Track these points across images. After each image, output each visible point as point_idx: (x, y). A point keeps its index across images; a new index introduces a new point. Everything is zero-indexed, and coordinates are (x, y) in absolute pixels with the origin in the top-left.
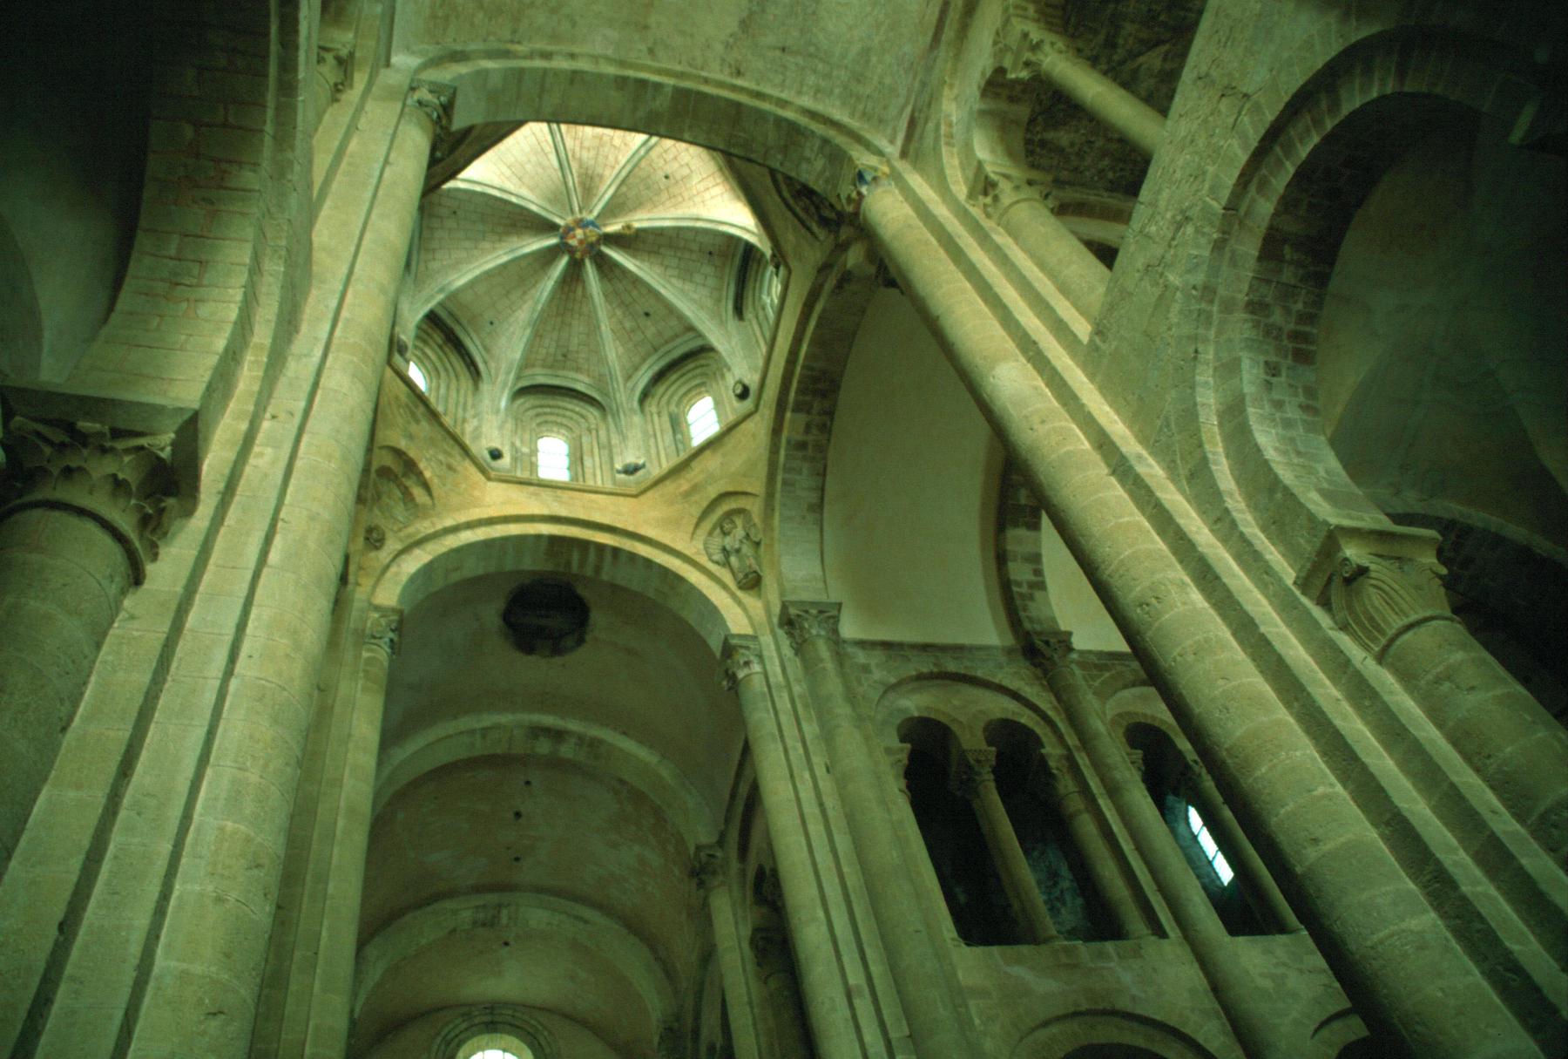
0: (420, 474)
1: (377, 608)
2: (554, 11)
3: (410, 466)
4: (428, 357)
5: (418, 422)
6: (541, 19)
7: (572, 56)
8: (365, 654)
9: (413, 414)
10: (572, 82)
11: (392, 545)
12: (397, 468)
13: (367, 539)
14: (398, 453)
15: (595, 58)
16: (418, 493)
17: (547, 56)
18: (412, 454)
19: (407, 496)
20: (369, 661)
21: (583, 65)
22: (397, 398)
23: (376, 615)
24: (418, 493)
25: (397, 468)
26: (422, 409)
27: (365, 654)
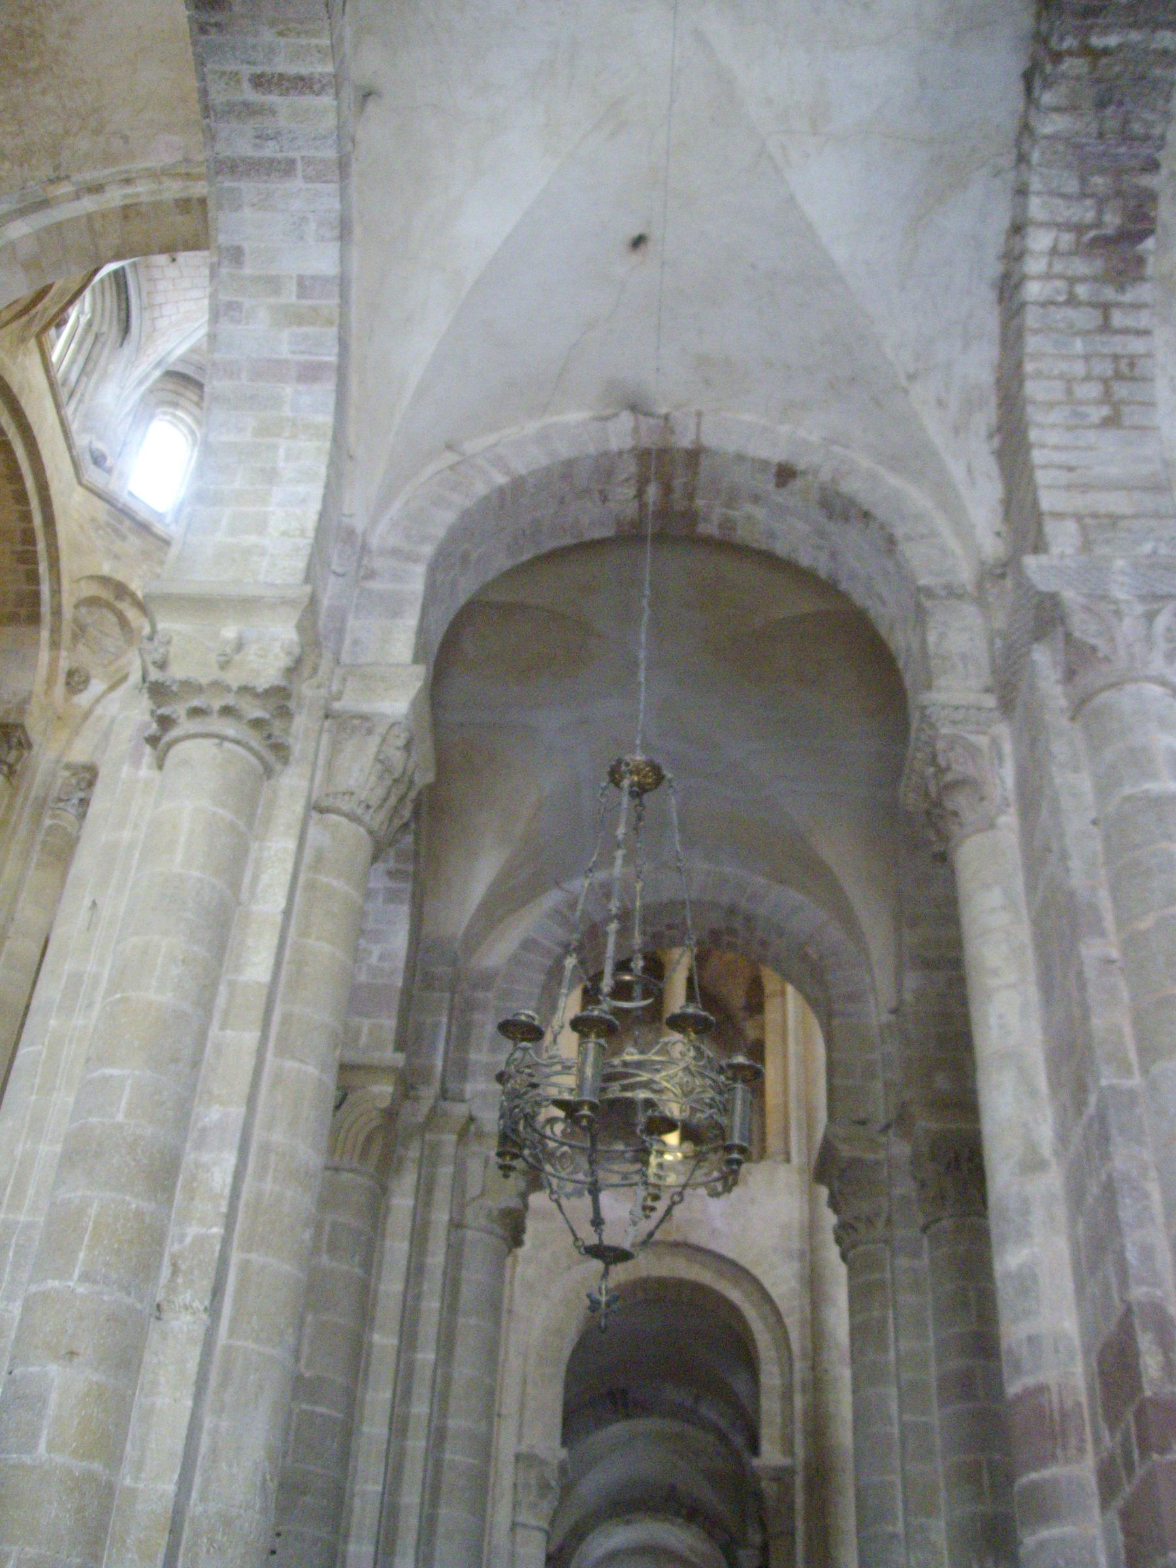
0: (133, 595)
1: (68, 767)
2: (97, 132)
3: (121, 590)
4: (182, 420)
5: (124, 538)
6: (83, 144)
7: (128, 181)
8: (48, 822)
9: (116, 531)
10: (126, 217)
11: (97, 686)
12: (105, 594)
13: (68, 684)
14: (105, 581)
15: (154, 175)
16: (132, 614)
17: (97, 189)
18: (119, 576)
19: (123, 622)
20: (51, 830)
21: (142, 190)
22: (93, 520)
23: (67, 774)
24: (132, 614)
25: (105, 594)
26: (127, 523)
27: (48, 822)
